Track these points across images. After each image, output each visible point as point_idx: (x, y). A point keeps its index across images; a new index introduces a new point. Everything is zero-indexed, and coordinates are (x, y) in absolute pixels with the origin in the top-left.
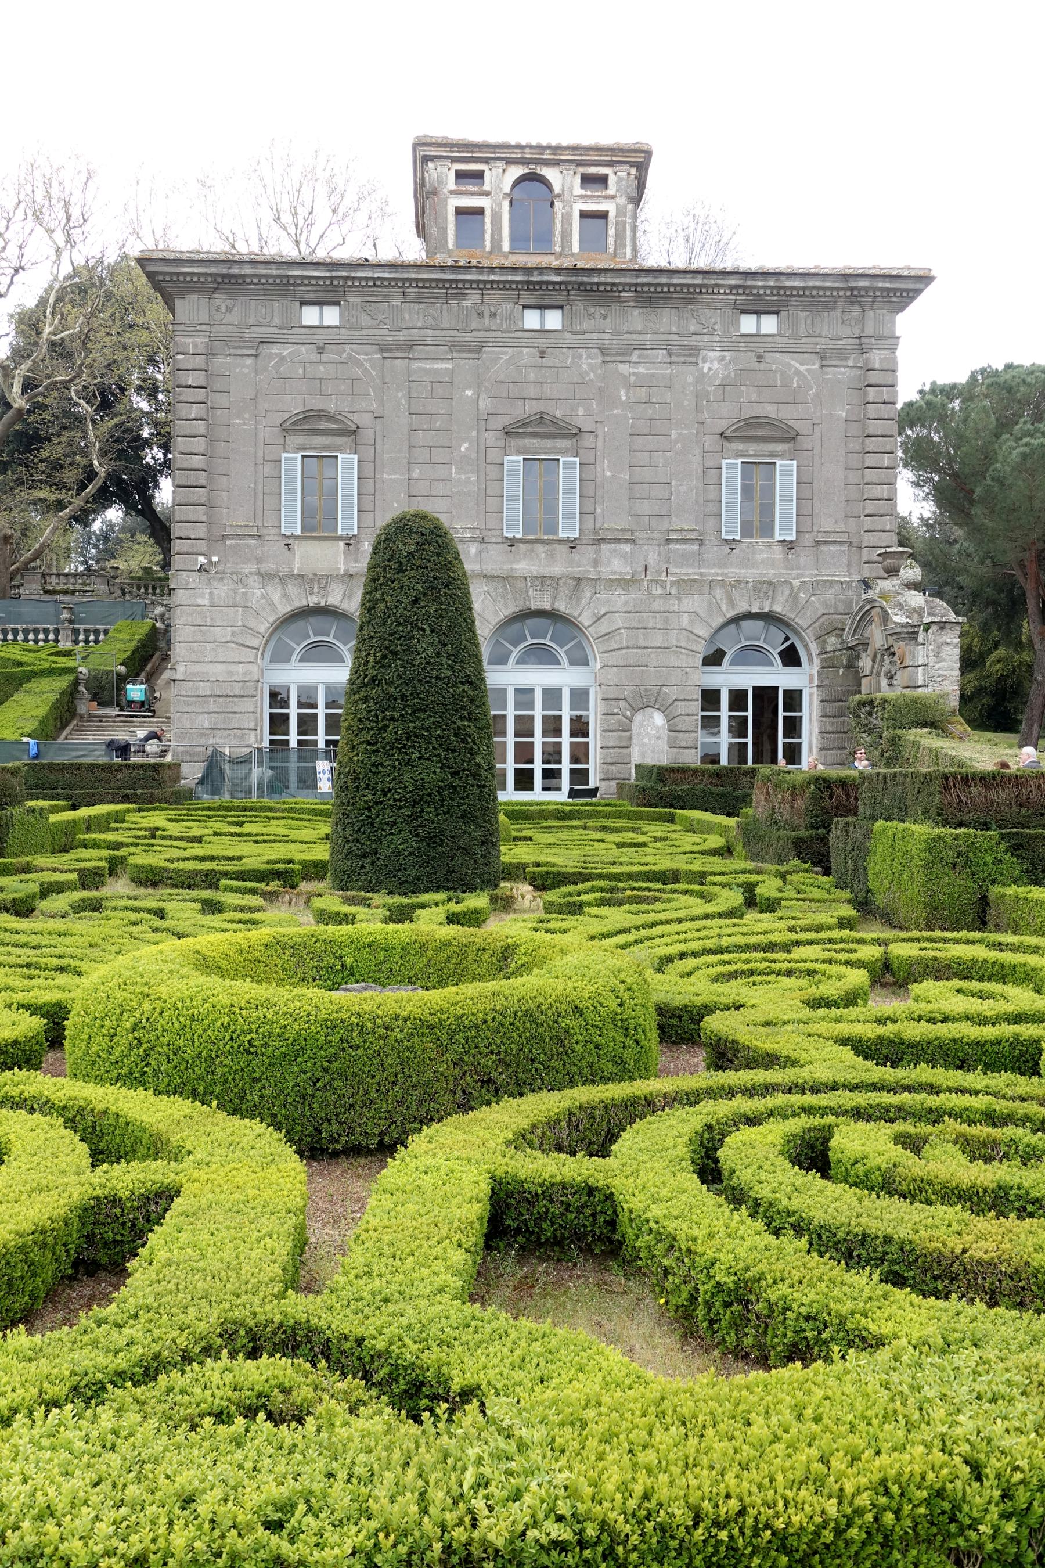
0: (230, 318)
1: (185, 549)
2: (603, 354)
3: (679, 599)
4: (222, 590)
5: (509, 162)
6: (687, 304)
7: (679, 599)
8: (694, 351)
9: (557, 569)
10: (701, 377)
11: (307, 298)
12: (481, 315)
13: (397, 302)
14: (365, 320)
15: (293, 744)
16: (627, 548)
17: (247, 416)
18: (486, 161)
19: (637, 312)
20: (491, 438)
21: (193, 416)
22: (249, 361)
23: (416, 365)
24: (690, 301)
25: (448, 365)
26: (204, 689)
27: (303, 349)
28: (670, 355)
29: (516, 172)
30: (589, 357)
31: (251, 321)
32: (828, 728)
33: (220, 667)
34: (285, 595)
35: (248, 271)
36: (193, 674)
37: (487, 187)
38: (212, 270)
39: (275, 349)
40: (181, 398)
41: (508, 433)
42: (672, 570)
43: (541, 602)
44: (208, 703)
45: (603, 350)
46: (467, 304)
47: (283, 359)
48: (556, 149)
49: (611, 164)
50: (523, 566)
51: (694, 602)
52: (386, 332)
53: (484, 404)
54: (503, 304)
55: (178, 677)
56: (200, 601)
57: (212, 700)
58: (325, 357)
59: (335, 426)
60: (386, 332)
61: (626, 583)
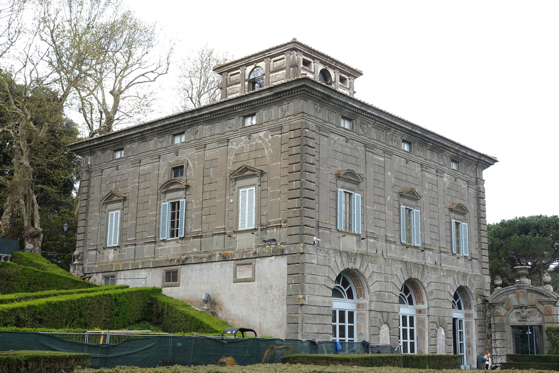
0: (320, 116)
1: (309, 232)
2: (422, 167)
3: (447, 278)
4: (321, 254)
5: (322, 62)
6: (441, 152)
7: (447, 278)
8: (443, 172)
9: (414, 260)
10: (444, 183)
11: (345, 115)
12: (392, 140)
13: (370, 126)
14: (361, 132)
15: (347, 341)
16: (431, 253)
17: (325, 166)
18: (314, 58)
19: (429, 151)
20: (396, 196)
21: (311, 162)
22: (326, 139)
23: (375, 156)
24: (442, 152)
25: (382, 159)
26: (315, 310)
27: (342, 138)
28: (437, 171)
29: (321, 67)
30: (418, 167)
31: (327, 119)
32: (480, 338)
33: (321, 299)
34: (342, 262)
35: (336, 97)
36: (311, 302)
37: (313, 70)
38: (326, 92)
39: (333, 136)
40: (308, 152)
41: (401, 195)
42: (442, 265)
43: (415, 275)
44: (316, 318)
45: (422, 165)
46: (388, 134)
47: (335, 141)
48: (337, 62)
49: (349, 75)
50: (406, 257)
51: (450, 280)
52: (367, 138)
53: (393, 180)
54: (399, 136)
55: (306, 303)
56: (314, 262)
57: (317, 316)
58: (349, 144)
59: (355, 179)
60: (367, 138)
61: (435, 269)
